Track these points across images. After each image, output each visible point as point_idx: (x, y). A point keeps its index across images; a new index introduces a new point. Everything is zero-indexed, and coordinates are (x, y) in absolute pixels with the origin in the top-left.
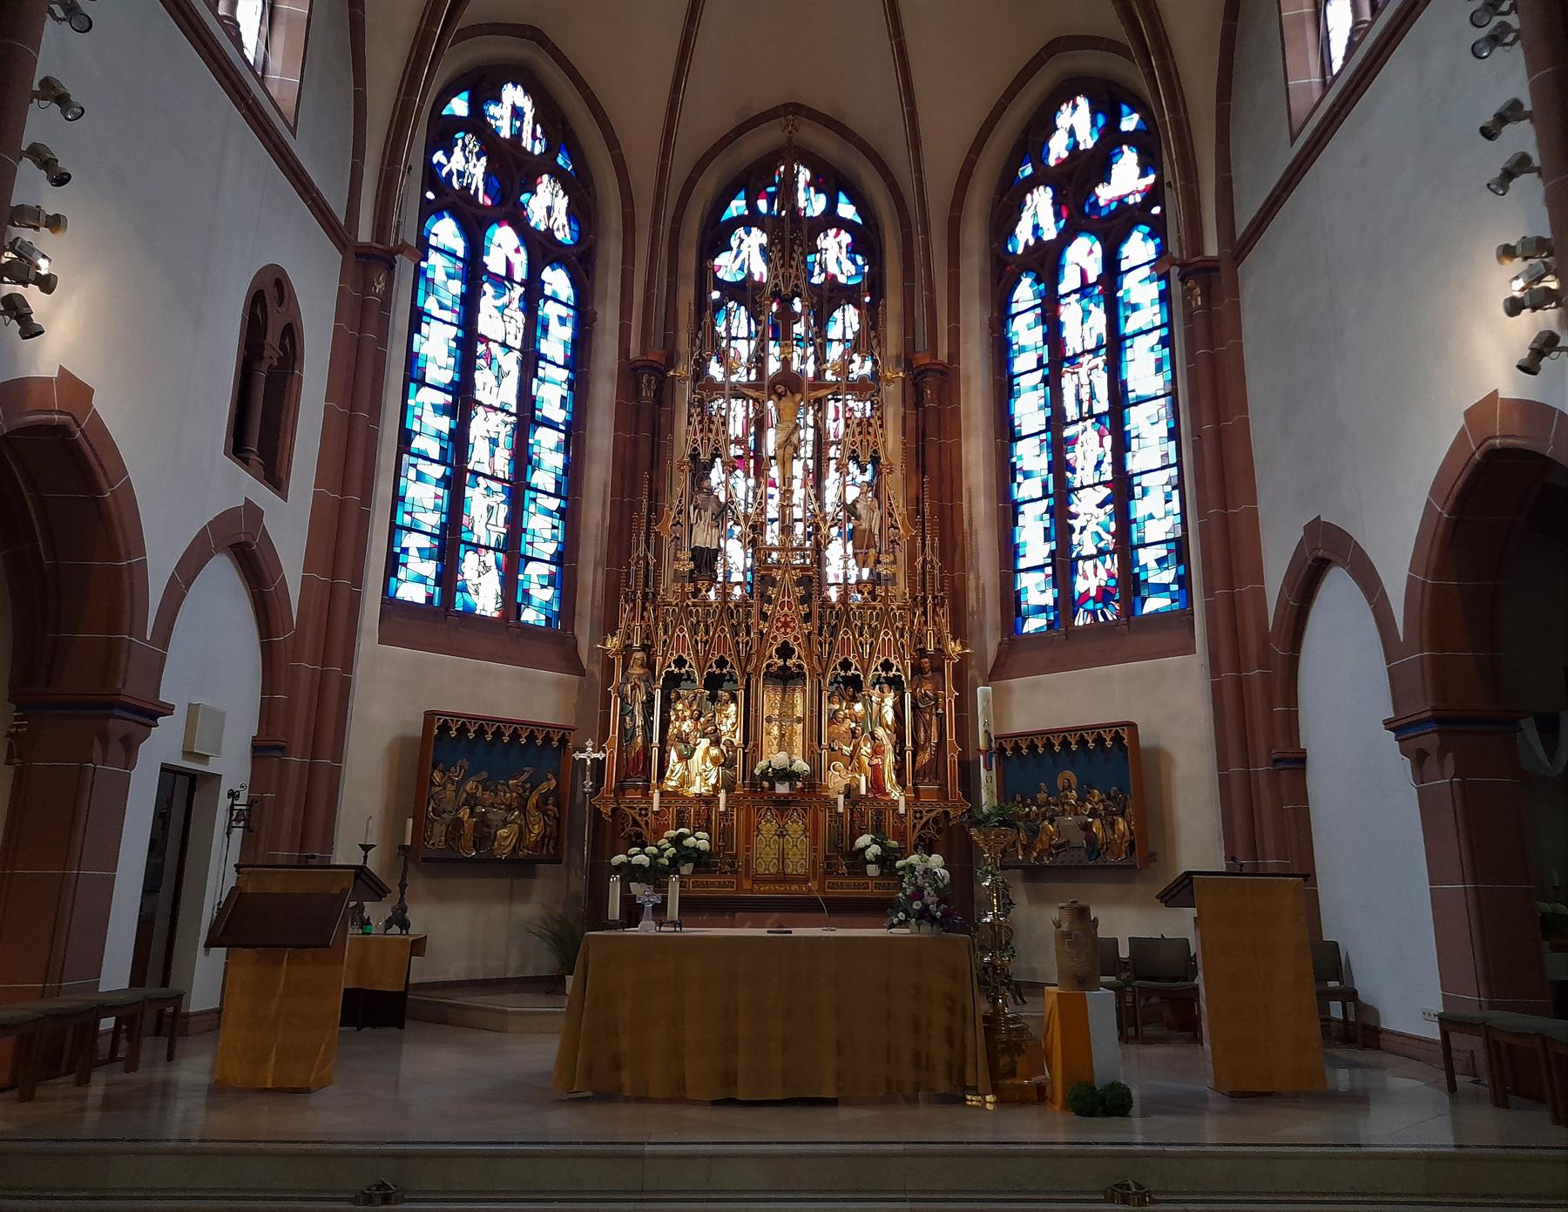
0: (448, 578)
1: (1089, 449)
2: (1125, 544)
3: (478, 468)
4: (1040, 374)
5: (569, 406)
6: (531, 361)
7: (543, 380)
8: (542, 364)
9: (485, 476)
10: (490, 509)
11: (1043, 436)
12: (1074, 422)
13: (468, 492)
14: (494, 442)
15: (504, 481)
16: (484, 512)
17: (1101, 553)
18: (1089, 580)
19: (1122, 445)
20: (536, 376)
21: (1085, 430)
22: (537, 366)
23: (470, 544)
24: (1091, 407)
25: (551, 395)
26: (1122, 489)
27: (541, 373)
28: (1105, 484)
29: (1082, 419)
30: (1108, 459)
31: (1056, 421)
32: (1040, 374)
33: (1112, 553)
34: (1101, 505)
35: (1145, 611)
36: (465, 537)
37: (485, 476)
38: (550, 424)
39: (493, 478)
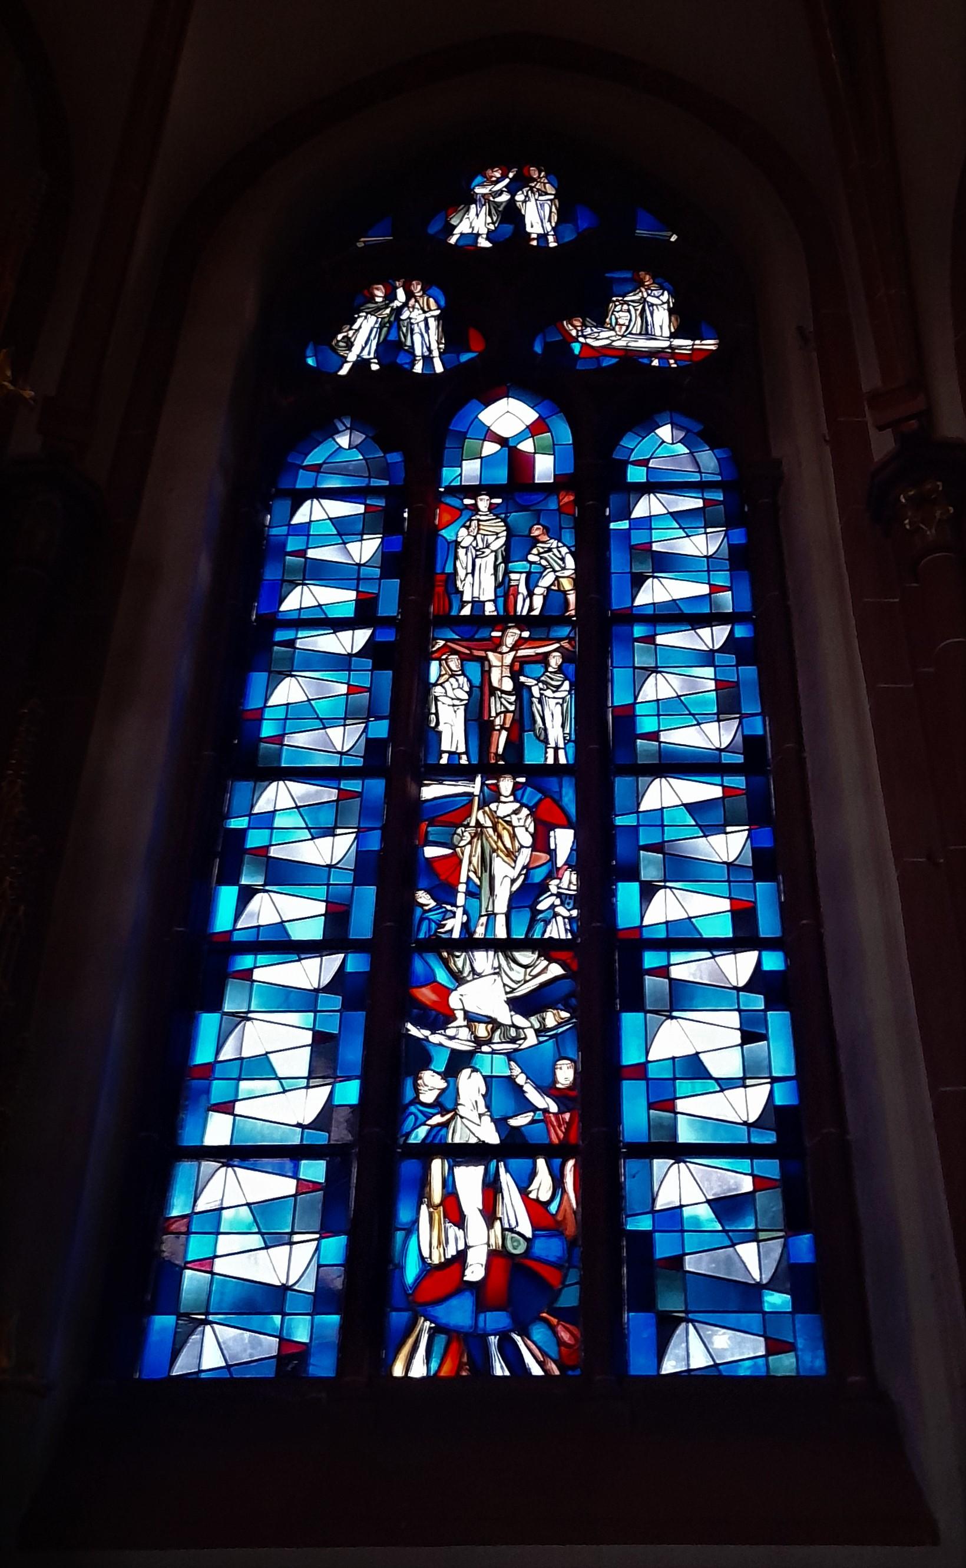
1: (503, 853)
2: (600, 1130)
4: (362, 636)
11: (353, 785)
12: (455, 771)
17: (514, 1147)
18: (469, 1225)
19: (606, 860)
21: (496, 796)
24: (515, 745)
26: (604, 978)
28: (548, 949)
29: (484, 767)
30: (569, 881)
31: (402, 749)
32: (362, 636)
33: (556, 1154)
34: (522, 1005)
35: (670, 1366)
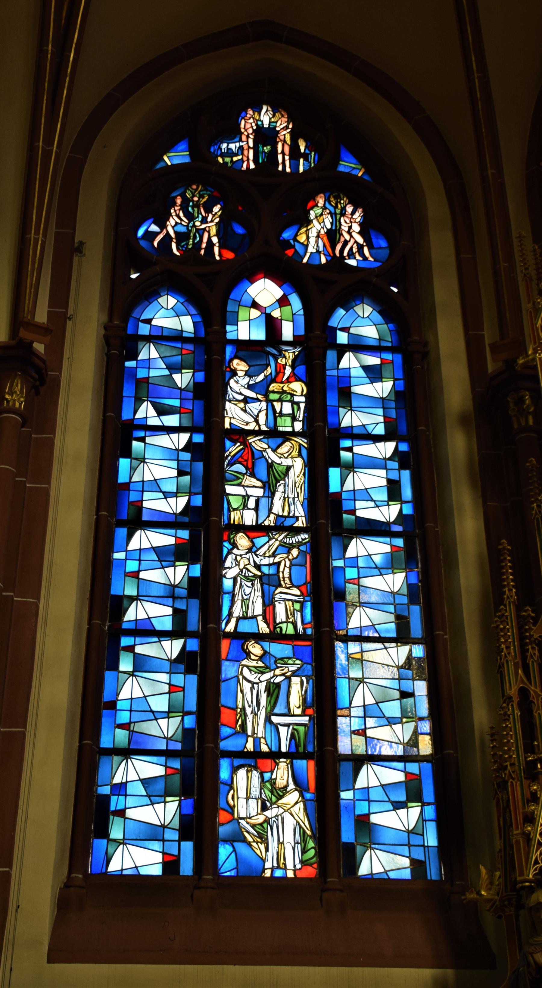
0: (203, 821)
3: (246, 627)
5: (407, 492)
6: (324, 445)
7: (350, 467)
8: (347, 443)
9: (258, 637)
10: (273, 690)
13: (228, 669)
14: (269, 582)
15: (296, 637)
16: (263, 699)
20: (336, 462)
22: (338, 449)
23: (242, 754)
25: (369, 485)
27: (345, 456)
36: (229, 745)
37: (258, 637)
38: (371, 529)
39: (275, 636)
